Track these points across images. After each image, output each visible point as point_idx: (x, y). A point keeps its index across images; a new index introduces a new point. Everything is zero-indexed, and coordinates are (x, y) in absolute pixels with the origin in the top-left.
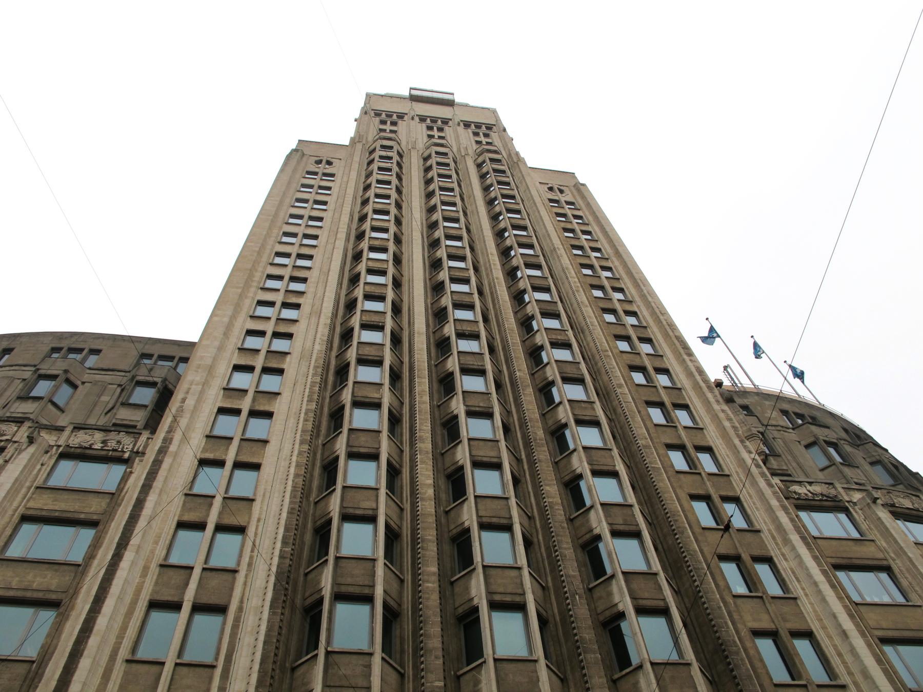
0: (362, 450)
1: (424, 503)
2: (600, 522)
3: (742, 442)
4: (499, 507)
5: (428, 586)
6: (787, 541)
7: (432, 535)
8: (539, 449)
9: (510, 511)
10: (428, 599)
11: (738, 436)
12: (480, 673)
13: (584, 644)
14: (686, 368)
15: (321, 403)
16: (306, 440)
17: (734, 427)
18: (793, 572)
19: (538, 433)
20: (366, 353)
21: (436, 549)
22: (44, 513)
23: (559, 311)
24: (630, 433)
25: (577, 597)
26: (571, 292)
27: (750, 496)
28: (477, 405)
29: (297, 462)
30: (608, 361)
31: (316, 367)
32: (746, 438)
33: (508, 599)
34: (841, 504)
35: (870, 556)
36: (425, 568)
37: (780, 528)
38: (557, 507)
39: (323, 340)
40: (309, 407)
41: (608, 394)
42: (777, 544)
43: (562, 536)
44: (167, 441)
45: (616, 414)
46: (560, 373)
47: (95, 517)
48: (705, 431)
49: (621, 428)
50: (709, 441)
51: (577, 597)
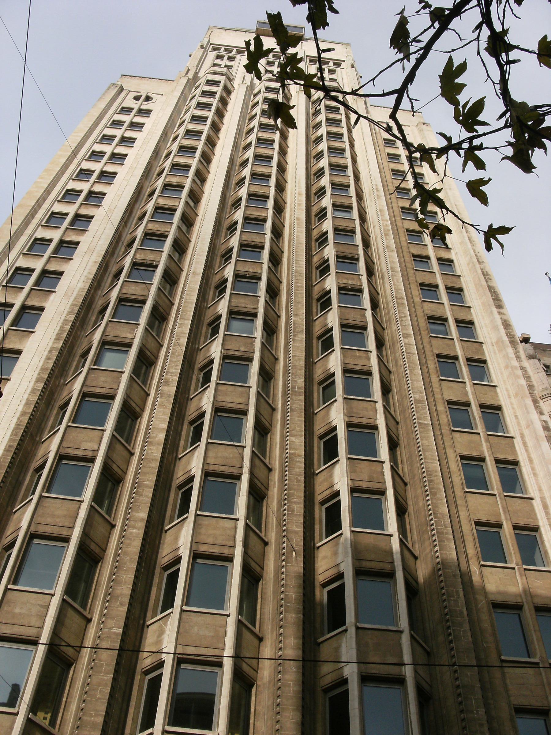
0: (99, 391)
1: (152, 448)
3: (535, 402)
4: (231, 456)
5: (132, 532)
7: (151, 481)
8: (294, 397)
9: (243, 460)
10: (129, 545)
12: (165, 624)
13: (288, 602)
14: (492, 321)
15: (72, 342)
16: (42, 378)
19: (299, 381)
20: (131, 291)
21: (151, 495)
23: (358, 255)
24: (406, 386)
25: (294, 554)
26: (380, 236)
28: (237, 349)
29: (28, 400)
30: (401, 308)
31: (73, 305)
32: (540, 398)
33: (215, 550)
36: (134, 514)
38: (297, 459)
39: (88, 278)
40: (55, 346)
41: (393, 344)
43: (295, 490)
45: (397, 365)
46: (341, 319)
49: (399, 381)
50: (499, 400)
51: (294, 554)
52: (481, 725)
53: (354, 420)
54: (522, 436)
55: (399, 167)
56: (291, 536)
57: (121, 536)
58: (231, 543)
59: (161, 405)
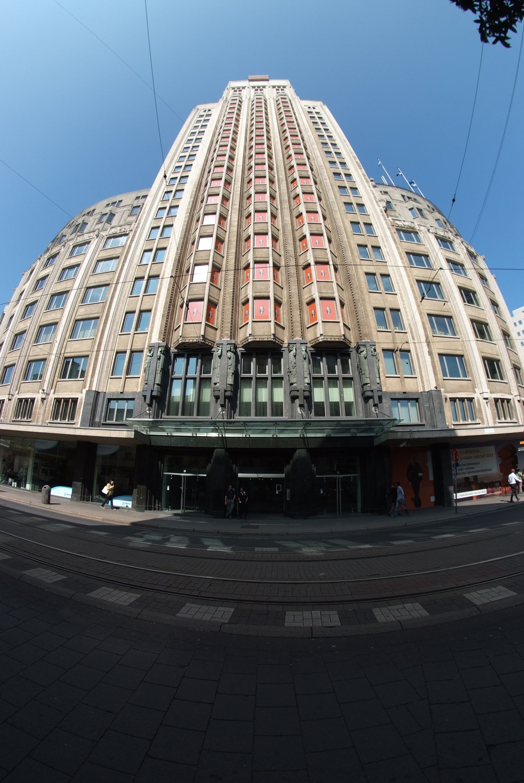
0: (210, 212)
2: (306, 229)
3: (377, 202)
6: (387, 241)
10: (230, 262)
11: (376, 200)
17: (375, 197)
18: (388, 253)
20: (215, 176)
22: (103, 258)
27: (376, 223)
31: (194, 185)
33: (262, 259)
34: (415, 230)
35: (422, 250)
37: (386, 236)
42: (383, 242)
44: (139, 224)
47: (118, 255)
48: (363, 198)
52: (362, 312)
53: (309, 210)
54: (373, 214)
55: (315, 121)
56: (289, 252)
57: (227, 259)
58: (267, 256)
59: (234, 213)
